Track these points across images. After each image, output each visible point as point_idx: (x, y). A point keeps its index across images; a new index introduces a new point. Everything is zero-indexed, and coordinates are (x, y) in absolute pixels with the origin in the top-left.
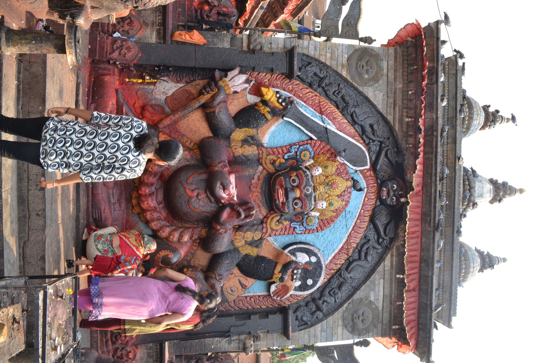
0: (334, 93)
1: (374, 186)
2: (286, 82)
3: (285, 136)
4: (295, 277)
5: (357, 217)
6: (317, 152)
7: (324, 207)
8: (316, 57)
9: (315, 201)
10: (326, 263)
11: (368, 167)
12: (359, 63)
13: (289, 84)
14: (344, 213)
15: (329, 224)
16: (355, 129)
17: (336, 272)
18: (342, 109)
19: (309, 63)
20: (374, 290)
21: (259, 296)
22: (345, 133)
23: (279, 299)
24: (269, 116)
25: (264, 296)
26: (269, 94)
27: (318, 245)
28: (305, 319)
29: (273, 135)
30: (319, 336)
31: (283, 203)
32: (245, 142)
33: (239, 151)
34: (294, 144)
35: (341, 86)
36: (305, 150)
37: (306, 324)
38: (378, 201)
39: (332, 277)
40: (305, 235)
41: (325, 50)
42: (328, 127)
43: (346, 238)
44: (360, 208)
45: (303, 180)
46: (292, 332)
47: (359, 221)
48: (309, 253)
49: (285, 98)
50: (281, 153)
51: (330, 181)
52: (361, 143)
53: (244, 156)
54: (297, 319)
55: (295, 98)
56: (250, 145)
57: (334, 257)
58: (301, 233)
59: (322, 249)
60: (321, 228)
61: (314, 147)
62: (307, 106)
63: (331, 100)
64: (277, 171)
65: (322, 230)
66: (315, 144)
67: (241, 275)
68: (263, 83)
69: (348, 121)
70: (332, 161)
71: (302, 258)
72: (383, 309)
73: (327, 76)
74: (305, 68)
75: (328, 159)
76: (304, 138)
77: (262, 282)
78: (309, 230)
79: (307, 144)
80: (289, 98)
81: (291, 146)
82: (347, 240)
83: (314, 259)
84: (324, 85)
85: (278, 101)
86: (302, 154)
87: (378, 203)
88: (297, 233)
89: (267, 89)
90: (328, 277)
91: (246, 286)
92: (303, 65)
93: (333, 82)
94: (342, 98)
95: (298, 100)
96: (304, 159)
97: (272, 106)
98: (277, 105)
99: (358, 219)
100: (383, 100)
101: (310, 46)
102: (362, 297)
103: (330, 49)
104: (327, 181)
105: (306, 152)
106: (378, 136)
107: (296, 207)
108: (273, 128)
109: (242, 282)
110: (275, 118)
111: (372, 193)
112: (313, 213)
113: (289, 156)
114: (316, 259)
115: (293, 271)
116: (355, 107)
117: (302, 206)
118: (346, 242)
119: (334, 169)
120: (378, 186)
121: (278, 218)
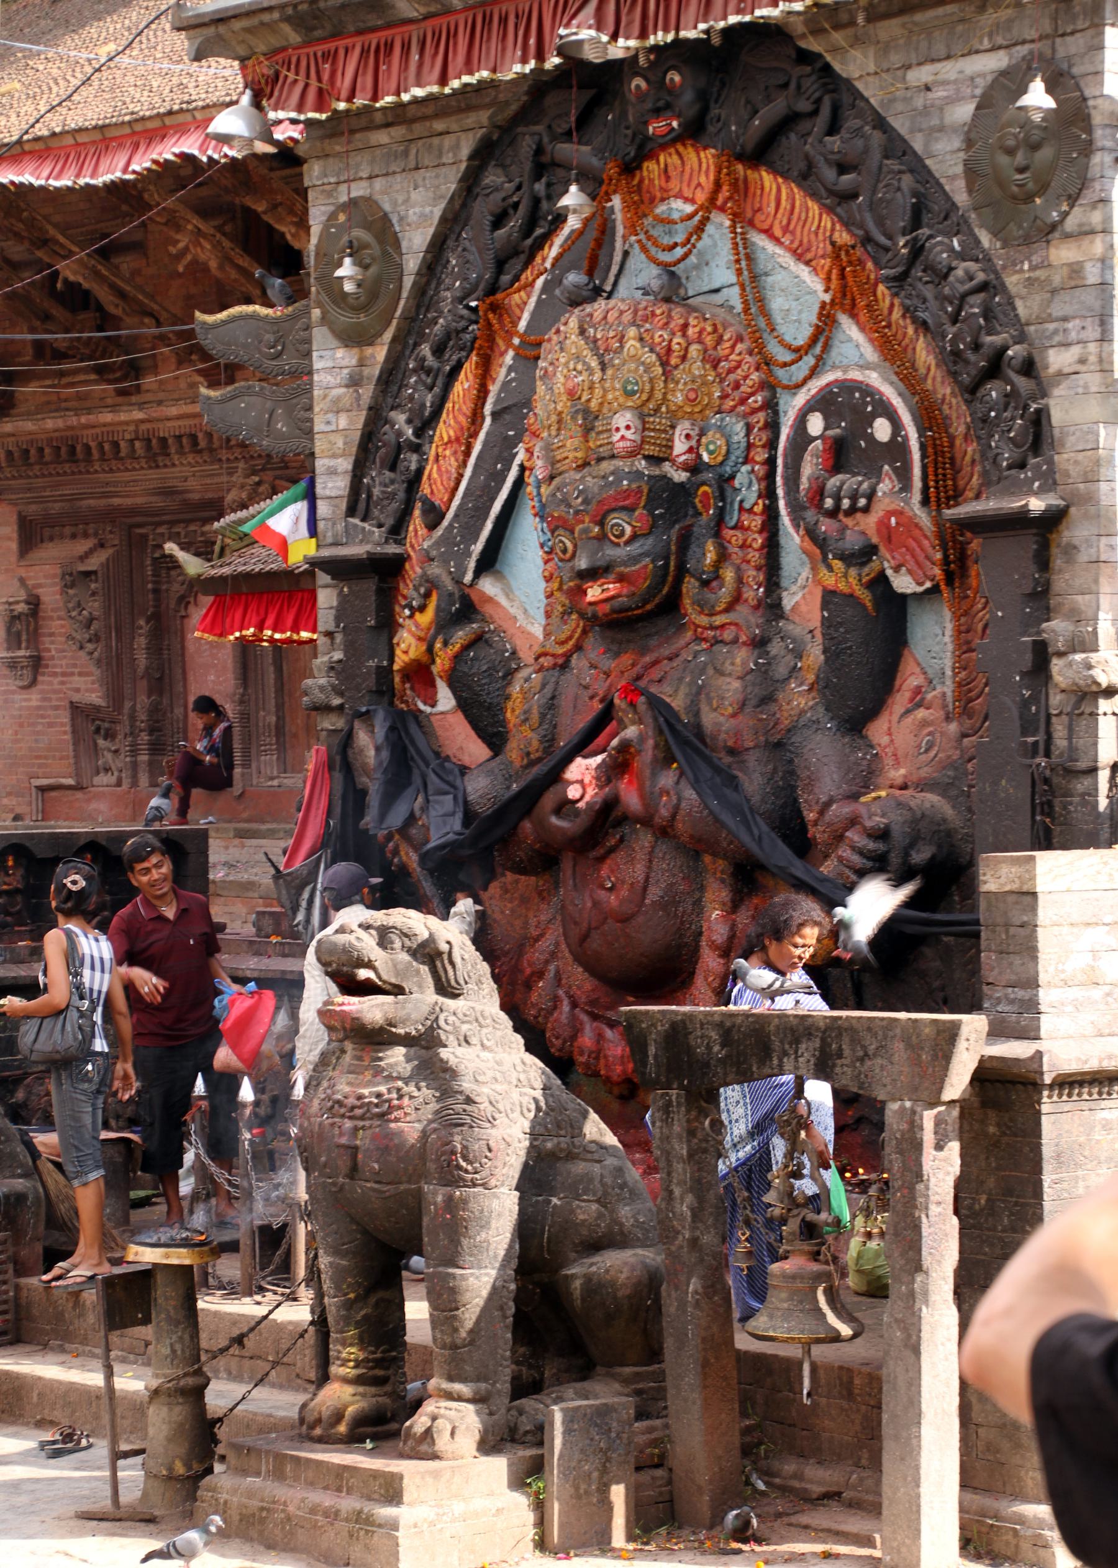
0: (431, 388)
8: (350, 467)
9: (613, 457)
18: (462, 349)
30: (1075, 351)
31: (621, 579)
41: (332, 437)
54: (1022, 465)
72: (1007, 47)
82: (807, 263)
83: (816, 424)
85: (422, 609)
91: (918, 691)
107: (628, 530)
115: (833, 513)
117: (623, 508)
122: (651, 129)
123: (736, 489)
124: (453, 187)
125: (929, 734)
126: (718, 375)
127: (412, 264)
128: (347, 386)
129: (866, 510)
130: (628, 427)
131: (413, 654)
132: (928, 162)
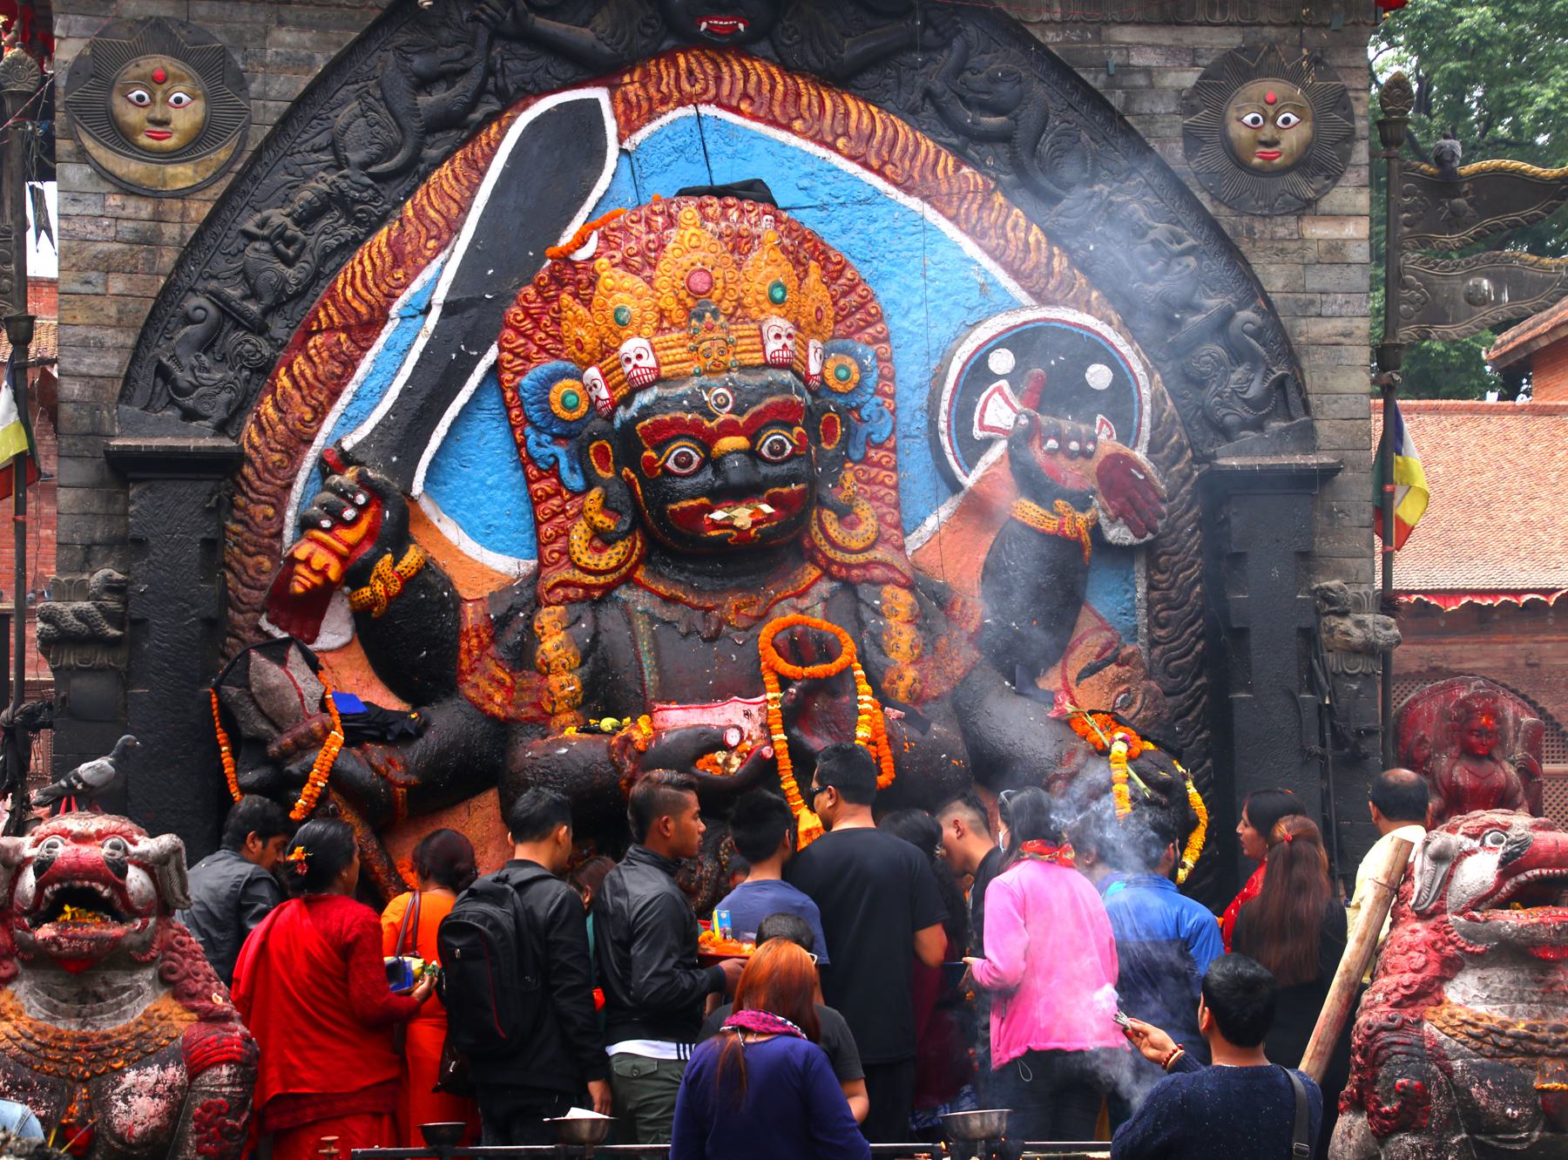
0: (289, 263)
1: (690, 72)
2: (253, 478)
3: (482, 482)
4: (1074, 446)
5: (822, 152)
6: (549, 343)
7: (784, 325)
8: (130, 341)
9: (766, 366)
10: (1022, 296)
11: (601, 94)
12: (144, 140)
13: (258, 464)
14: (809, 219)
15: (852, 289)
16: (440, 165)
17: (1067, 250)
18: (359, 222)
19: (162, 372)
20: (1147, 71)
21: (1151, 587)
22: (464, 210)
23: (1164, 508)
24: (412, 558)
25: (1152, 566)
26: (317, 557)
27: (942, 331)
28: (1254, 390)
29: (485, 534)
32: (523, 656)
33: (566, 684)
34: (520, 445)
35: (250, 226)
36: (547, 401)
37: (1281, 383)
38: (755, 48)
39: (1085, 266)
40: (903, 392)
41: (96, 301)
42: (440, 296)
43: (913, 203)
44: (782, 136)
45: (677, 422)
46: (1313, 449)
47: (840, 143)
48: (978, 374)
49: (333, 489)
50: (556, 501)
51: (680, 301)
52: (503, 132)
53: (581, 665)
54: (1258, 426)
55: (319, 442)
56: (531, 638)
57: (996, 259)
58: (893, 413)
59: (959, 315)
60: (869, 325)
61: (528, 359)
62: (352, 387)
63: (317, 276)
64: (638, 523)
65: (879, 317)
66: (517, 355)
67: (1059, 664)
68: (267, 580)
69: (410, 194)
70: (592, 284)
71: (999, 411)
73: (215, 296)
74: (185, 393)
75: (587, 303)
76: (491, 401)
77: (1092, 576)
78: (881, 376)
79: (516, 390)
80: (326, 467)
81: (524, 459)
82: (924, 198)
83: (1002, 361)
84: (253, 307)
86: (565, 415)
87: (764, 46)
88: (893, 431)
89: (301, 569)
90: (1082, 280)
92: (172, 402)
93: (237, 264)
94: (306, 219)
95: (328, 425)
96: (584, 407)
97: (368, 548)
98: (363, 526)
99: (832, 147)
100: (301, 26)
101: (83, 369)
102: (1178, 129)
103: (93, 275)
104: (677, 314)
105: (552, 396)
106: (468, 54)
107: (789, 448)
108: (451, 531)
109: (1092, 660)
110: (415, 531)
111: (719, 79)
112: (814, 368)
113: (572, 469)
114: (1005, 351)
116: (340, 164)
118: (933, 206)
119: (630, 281)
120: (685, 52)
121: (829, 517)
122: (704, 25)
123: (861, 420)
124: (355, 35)
125: (1128, 691)
126: (832, 297)
127: (268, 113)
128: (127, 242)
129: (1088, 455)
130: (789, 336)
131: (333, 573)
132: (1128, 119)
